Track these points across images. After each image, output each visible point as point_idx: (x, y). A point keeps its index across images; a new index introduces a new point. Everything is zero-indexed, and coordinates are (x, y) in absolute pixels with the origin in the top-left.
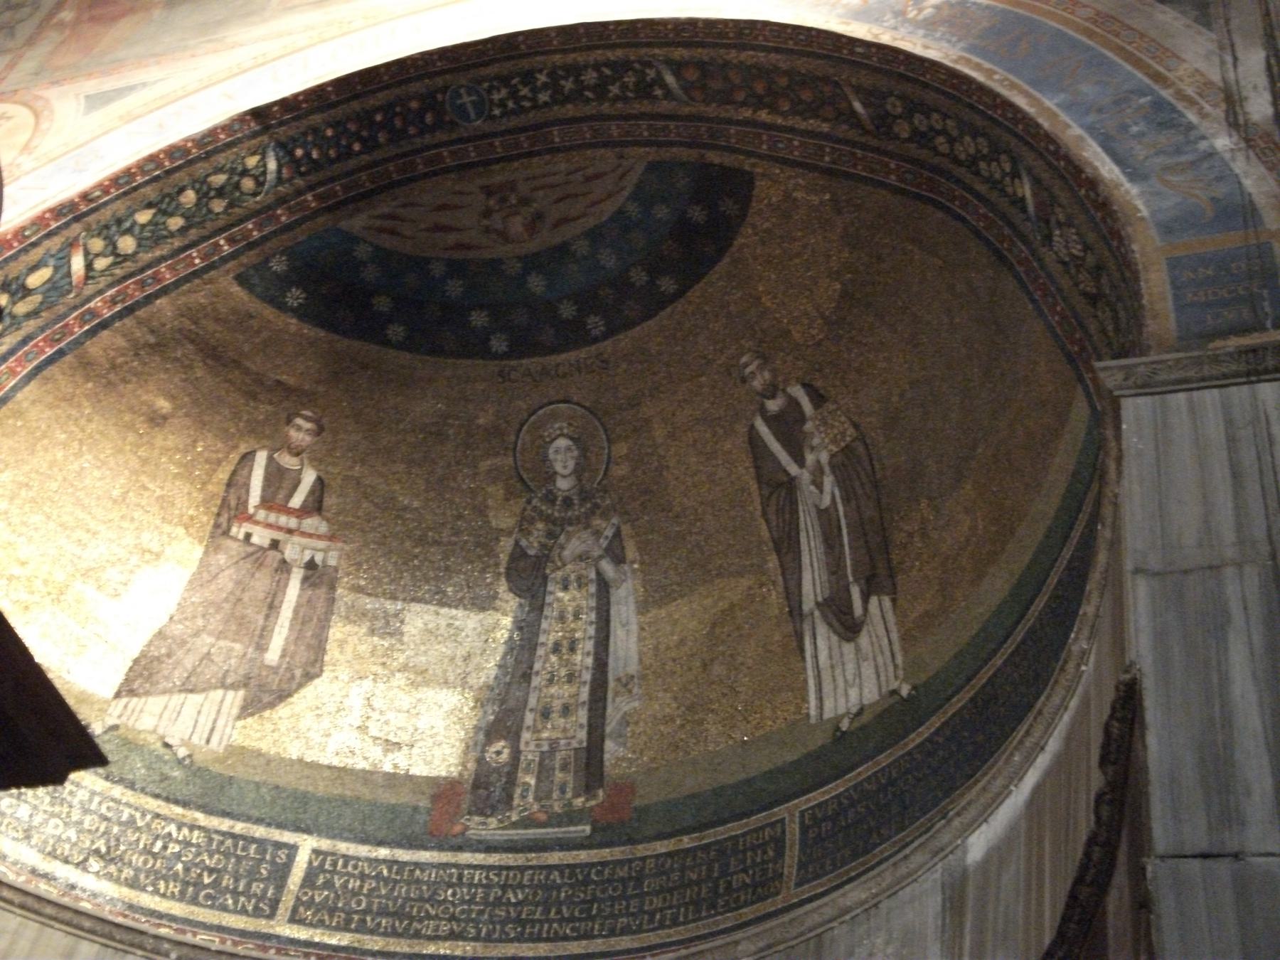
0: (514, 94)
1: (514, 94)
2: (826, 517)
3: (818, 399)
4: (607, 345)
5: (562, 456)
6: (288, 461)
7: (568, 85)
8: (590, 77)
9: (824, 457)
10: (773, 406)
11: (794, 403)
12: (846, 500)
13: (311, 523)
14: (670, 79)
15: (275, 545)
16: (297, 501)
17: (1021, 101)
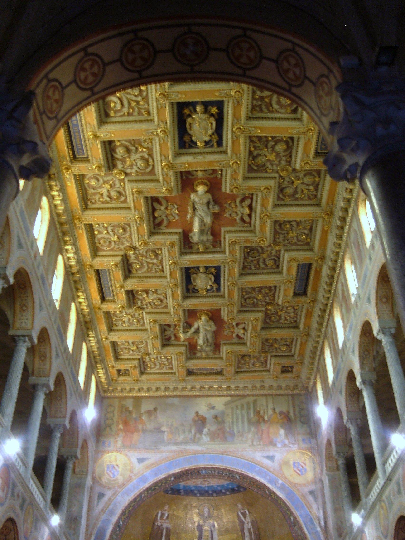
0: (212, 472)
1: (212, 472)
2: (249, 530)
3: (249, 512)
4: (216, 498)
5: (206, 511)
6: (164, 512)
7: (221, 473)
8: (225, 473)
9: (249, 521)
10: (242, 511)
11: (246, 512)
12: (253, 528)
13: (167, 521)
14: (238, 477)
15: (161, 525)
16: (165, 518)
17: (294, 512)
